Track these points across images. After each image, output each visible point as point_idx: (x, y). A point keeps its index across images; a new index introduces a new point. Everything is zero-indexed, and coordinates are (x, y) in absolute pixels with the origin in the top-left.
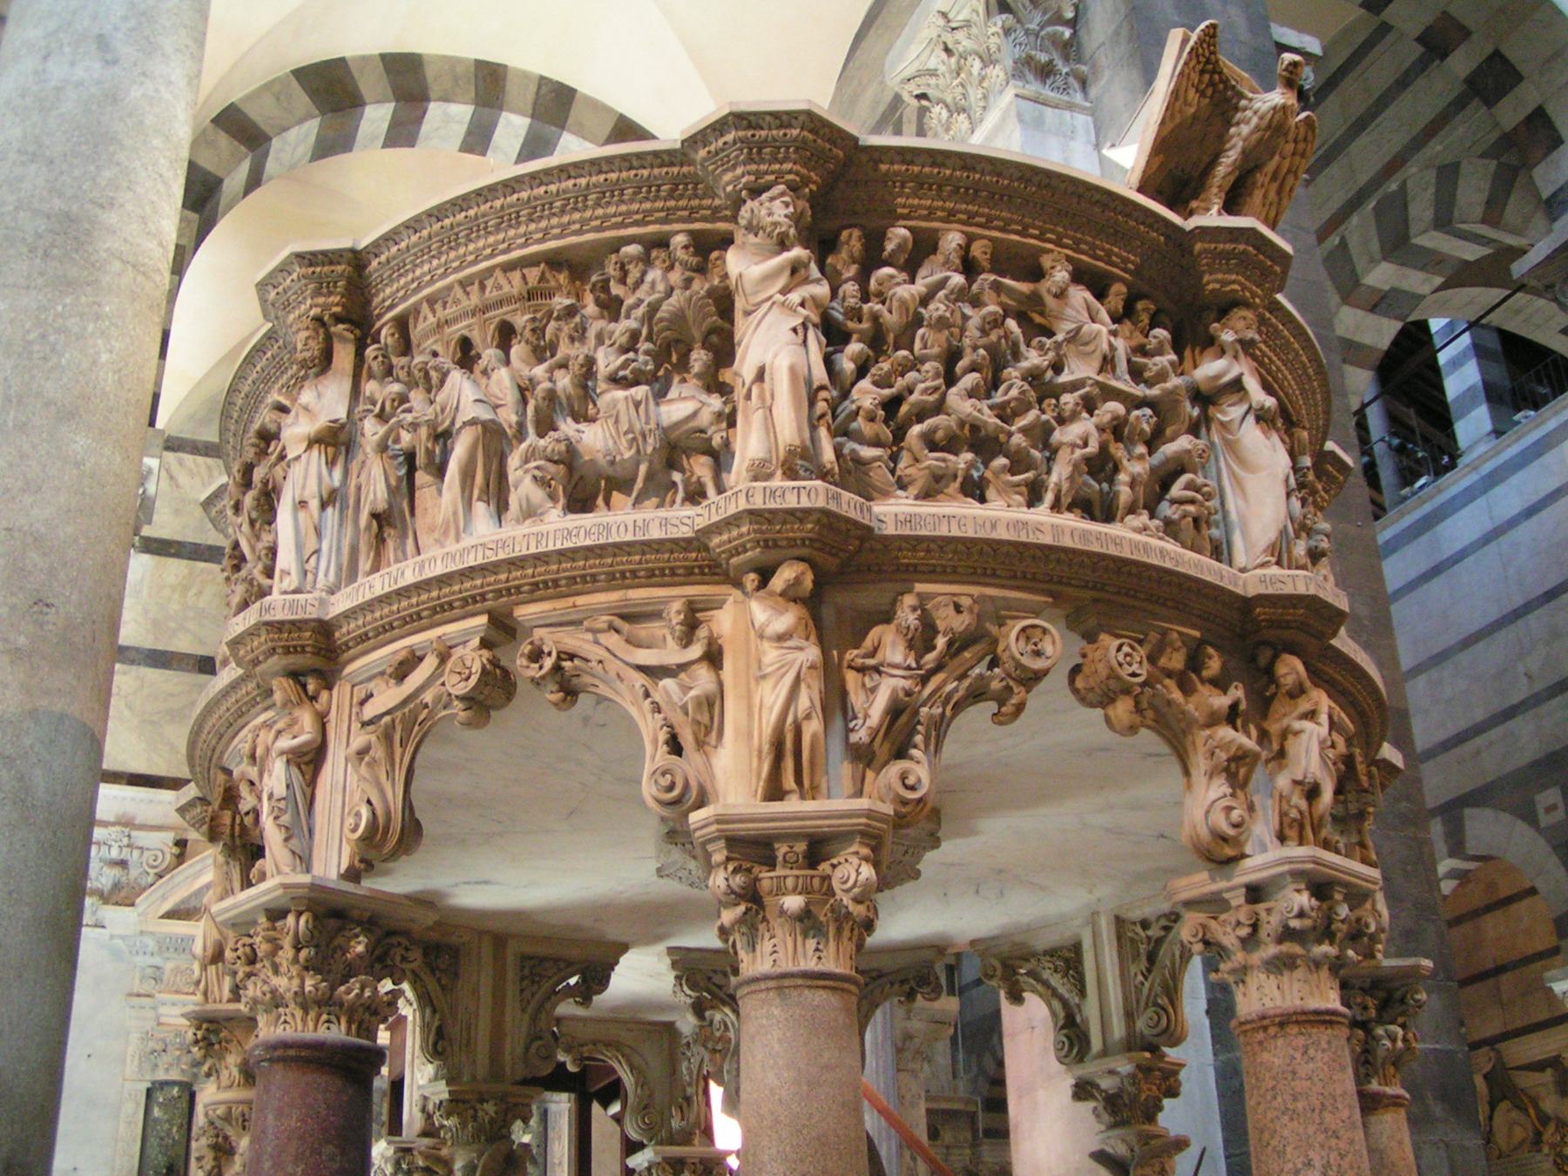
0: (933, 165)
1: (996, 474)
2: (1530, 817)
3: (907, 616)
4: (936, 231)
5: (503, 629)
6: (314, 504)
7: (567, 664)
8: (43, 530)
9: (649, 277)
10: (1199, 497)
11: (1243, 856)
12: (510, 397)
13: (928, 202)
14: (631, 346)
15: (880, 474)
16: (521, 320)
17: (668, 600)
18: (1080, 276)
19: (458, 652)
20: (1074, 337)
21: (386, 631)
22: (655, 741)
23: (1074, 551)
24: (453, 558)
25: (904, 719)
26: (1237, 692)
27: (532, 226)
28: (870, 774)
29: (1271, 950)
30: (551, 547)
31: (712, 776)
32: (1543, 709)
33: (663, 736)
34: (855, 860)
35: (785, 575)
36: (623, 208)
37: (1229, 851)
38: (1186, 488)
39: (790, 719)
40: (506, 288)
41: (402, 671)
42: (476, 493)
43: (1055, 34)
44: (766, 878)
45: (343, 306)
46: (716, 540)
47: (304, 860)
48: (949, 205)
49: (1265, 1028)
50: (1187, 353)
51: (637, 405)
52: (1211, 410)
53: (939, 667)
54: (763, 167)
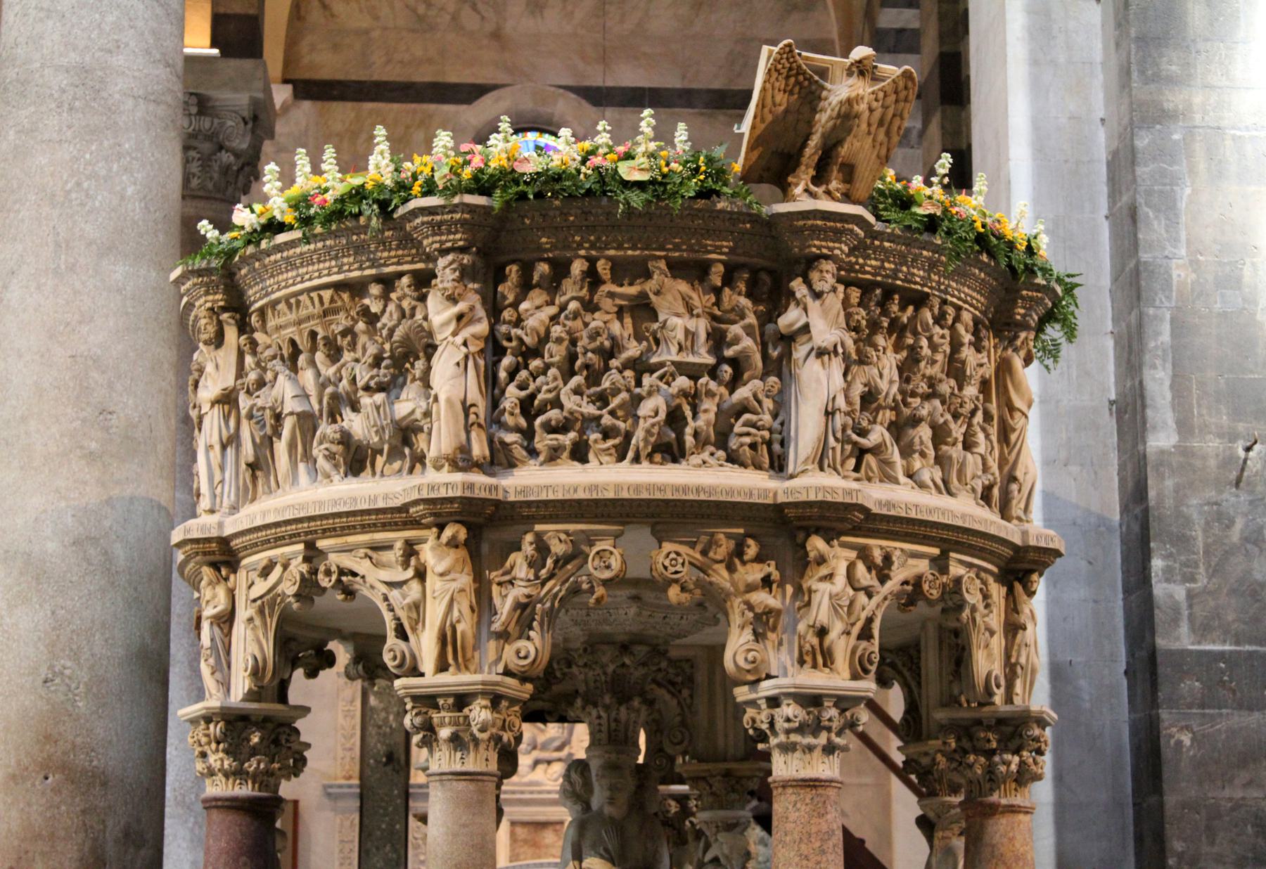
3: (528, 548)
5: (312, 554)
6: (217, 448)
7: (344, 579)
8: (99, 352)
9: (388, 309)
10: (753, 431)
14: (377, 361)
15: (519, 452)
17: (395, 540)
18: (677, 269)
19: (294, 563)
21: (255, 547)
27: (321, 266)
35: (448, 532)
38: (744, 425)
41: (266, 572)
44: (435, 716)
45: (226, 301)
46: (412, 510)
47: (226, 685)
51: (378, 408)
53: (551, 576)
54: (444, 238)
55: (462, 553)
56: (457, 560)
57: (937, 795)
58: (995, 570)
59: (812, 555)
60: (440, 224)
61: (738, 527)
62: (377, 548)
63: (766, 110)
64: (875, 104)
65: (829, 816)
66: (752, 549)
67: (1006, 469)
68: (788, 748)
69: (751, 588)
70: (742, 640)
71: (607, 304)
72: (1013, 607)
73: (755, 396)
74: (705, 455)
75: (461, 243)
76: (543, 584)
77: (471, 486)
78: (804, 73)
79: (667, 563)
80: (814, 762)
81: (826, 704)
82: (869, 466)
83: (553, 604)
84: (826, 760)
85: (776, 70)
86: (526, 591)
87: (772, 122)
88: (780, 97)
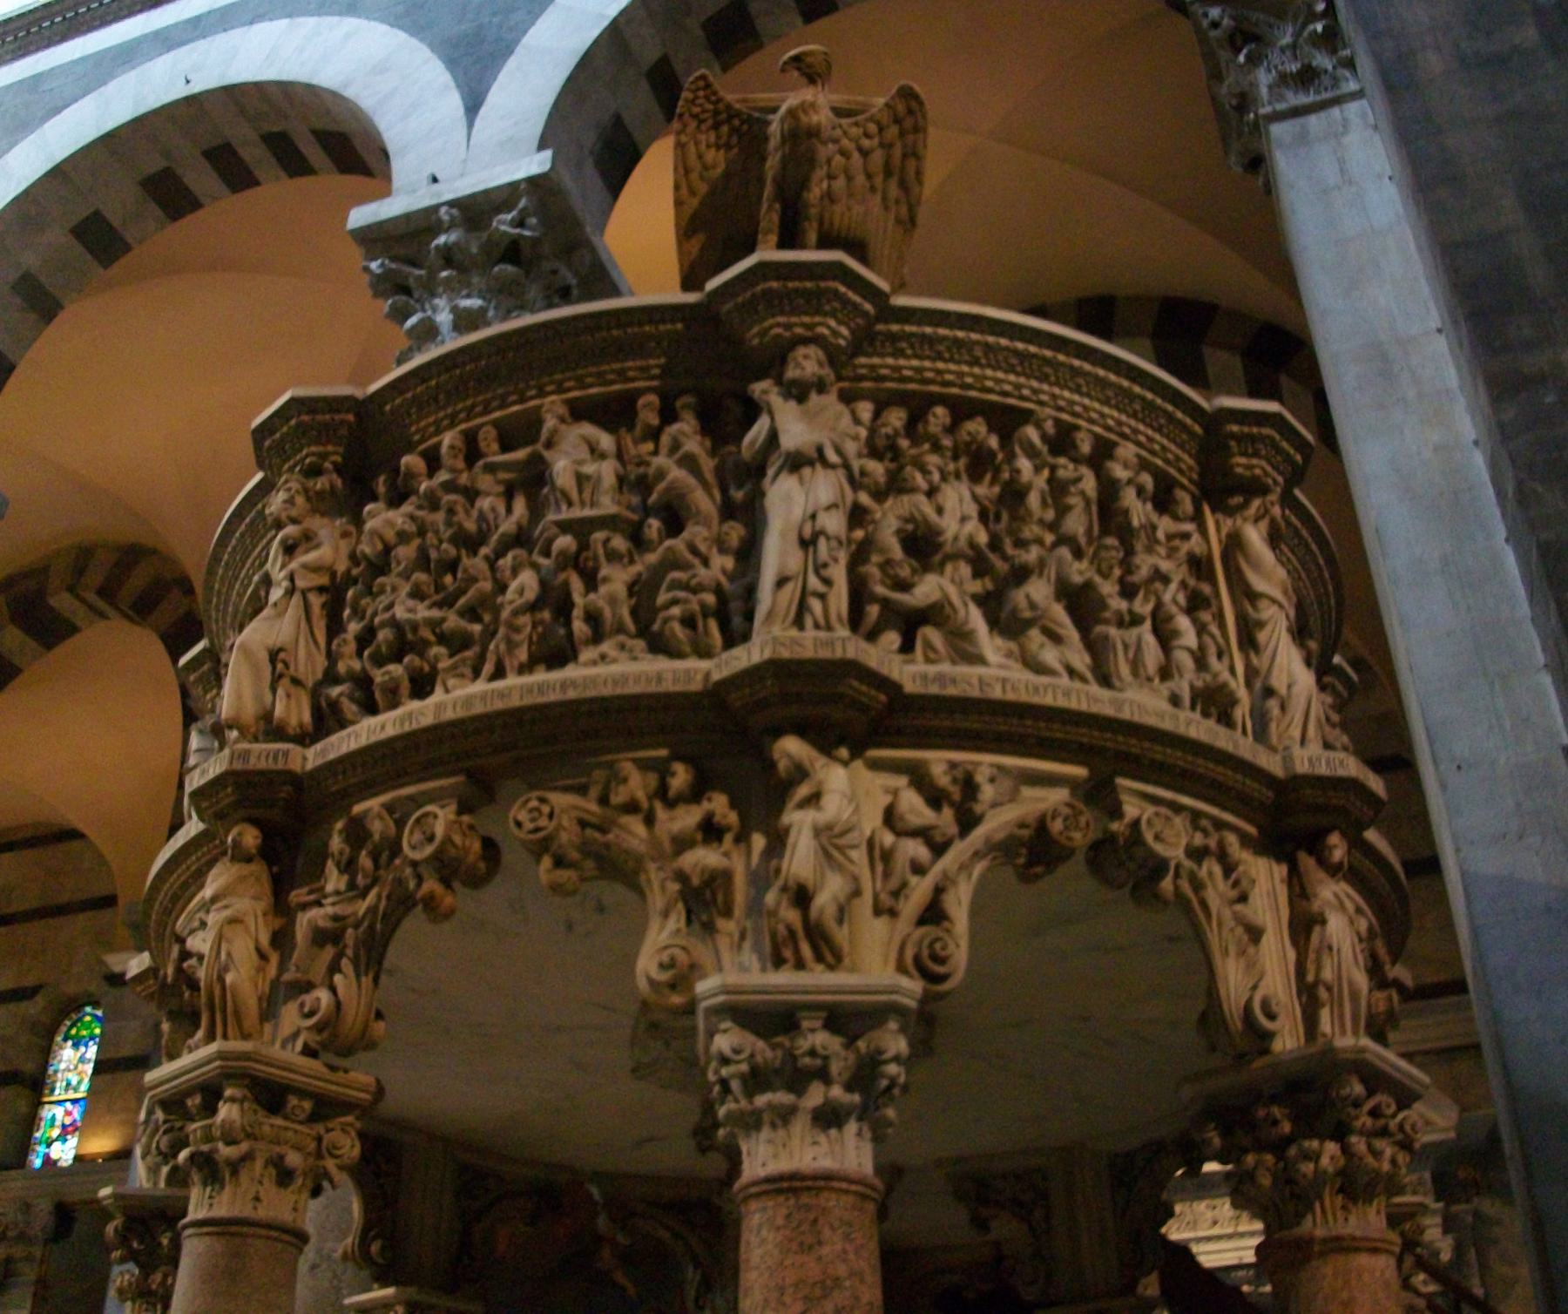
3: (336, 843)
10: (681, 594)
13: (431, 419)
15: (350, 708)
18: (579, 412)
26: (718, 804)
38: (671, 587)
43: (1310, 34)
48: (449, 411)
55: (258, 868)
56: (242, 879)
58: (1251, 830)
59: (782, 765)
61: (657, 746)
63: (694, 176)
64: (866, 143)
65: (825, 1251)
66: (681, 777)
67: (1258, 685)
68: (752, 1122)
69: (682, 844)
70: (665, 934)
71: (485, 482)
72: (1299, 890)
73: (694, 550)
74: (607, 647)
76: (363, 895)
77: (245, 755)
78: (738, 114)
79: (523, 816)
80: (796, 1141)
81: (805, 1024)
82: (928, 645)
83: (371, 927)
84: (822, 1138)
85: (695, 116)
86: (330, 910)
87: (712, 193)
88: (710, 155)
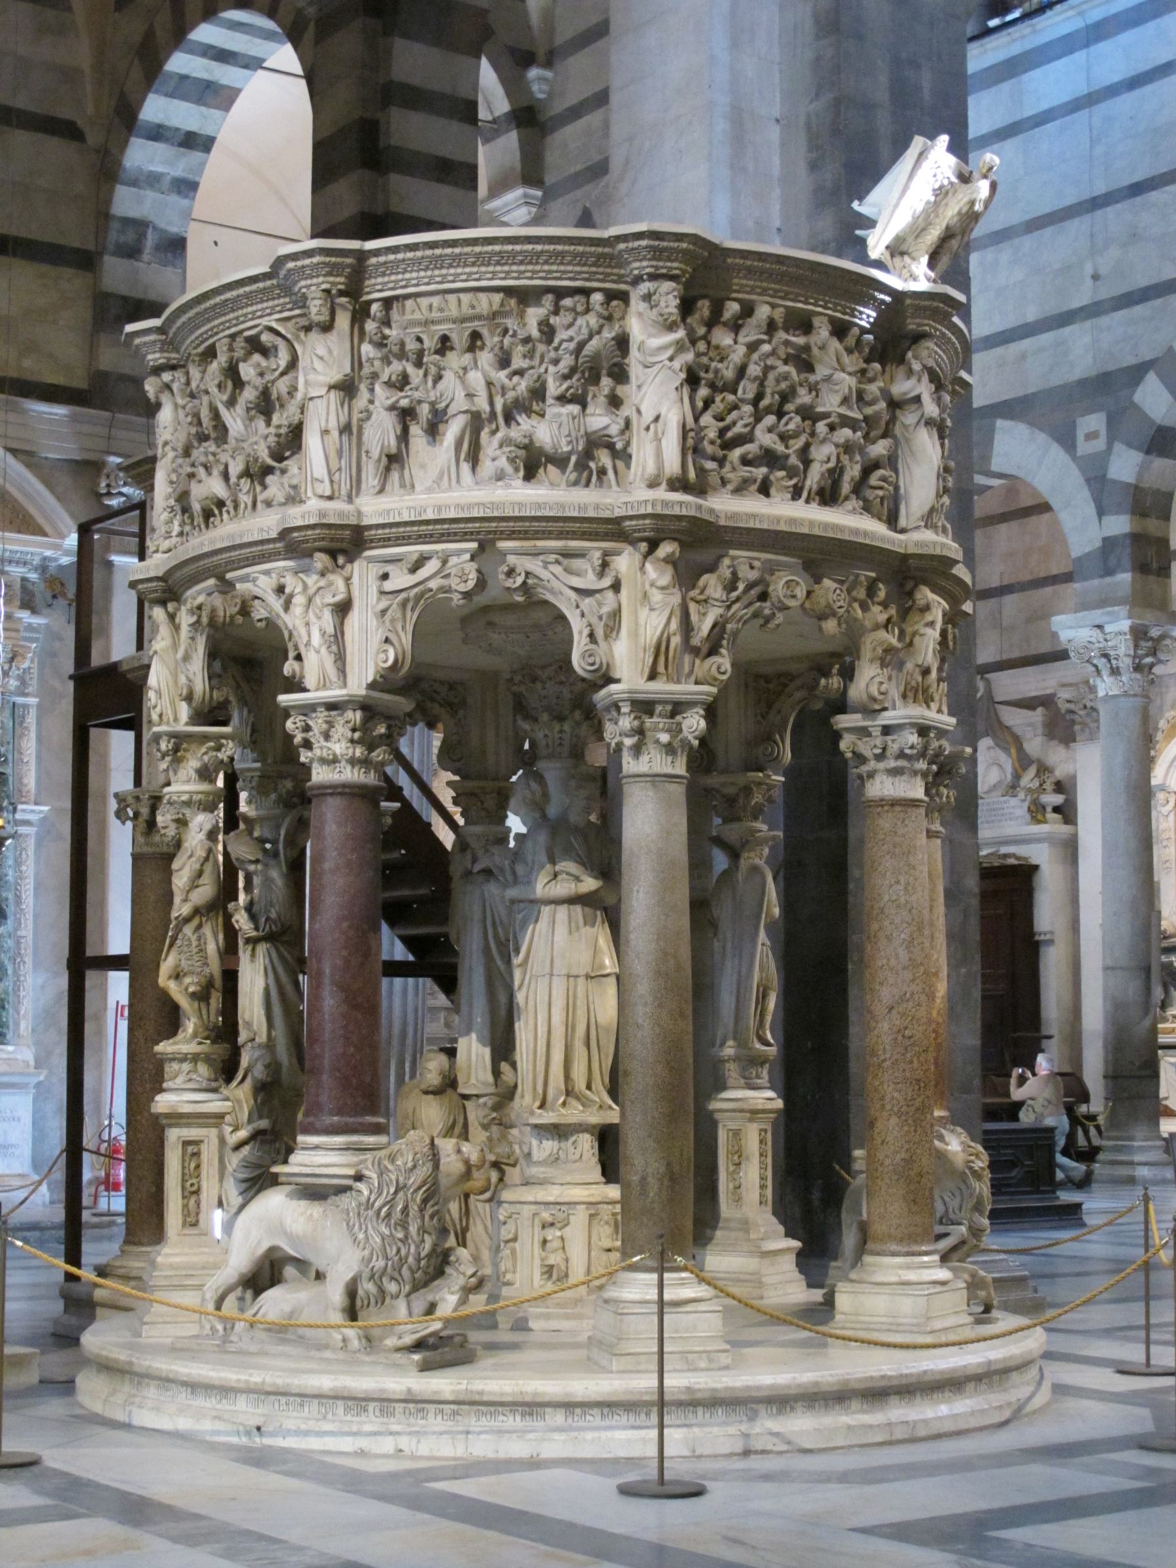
0: (759, 260)
1: (778, 480)
2: (1066, 439)
4: (752, 301)
6: (335, 434)
7: (530, 581)
11: (885, 709)
12: (482, 393)
13: (751, 283)
15: (714, 479)
16: (491, 340)
19: (453, 561)
20: (828, 379)
22: (580, 633)
23: (819, 537)
24: (463, 509)
25: (717, 629)
26: (893, 611)
27: (499, 268)
28: (698, 662)
29: (892, 763)
30: (528, 514)
31: (613, 656)
32: (1104, 320)
33: (586, 632)
34: (697, 717)
35: (666, 549)
36: (562, 268)
37: (877, 707)
39: (665, 635)
40: (478, 310)
42: (463, 456)
44: (649, 722)
46: (628, 523)
48: (765, 284)
49: (882, 806)
50: (888, 368)
51: (574, 418)
52: (898, 412)
53: (738, 599)
57: (739, 819)
60: (665, 249)
62: (567, 555)
75: (677, 272)
